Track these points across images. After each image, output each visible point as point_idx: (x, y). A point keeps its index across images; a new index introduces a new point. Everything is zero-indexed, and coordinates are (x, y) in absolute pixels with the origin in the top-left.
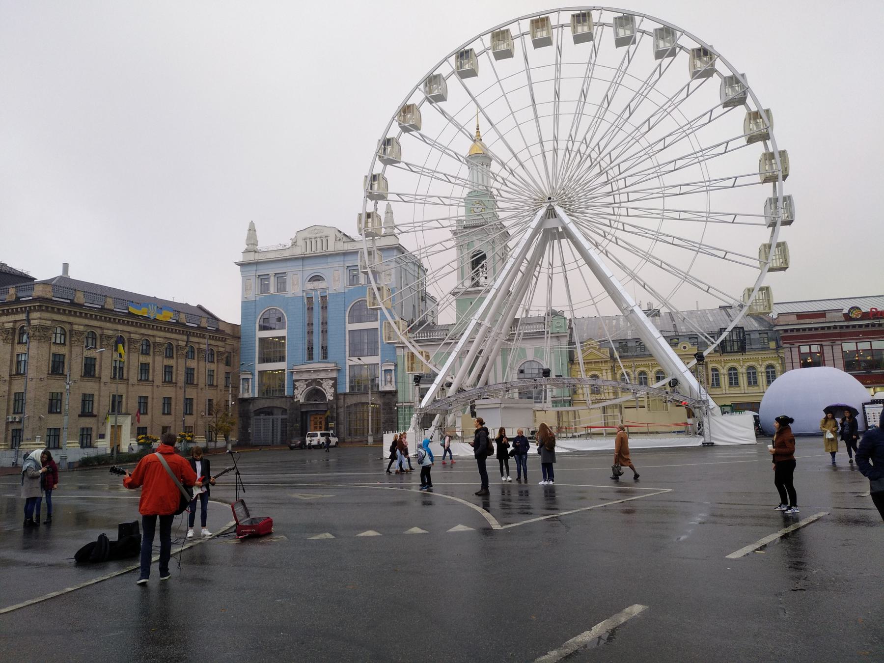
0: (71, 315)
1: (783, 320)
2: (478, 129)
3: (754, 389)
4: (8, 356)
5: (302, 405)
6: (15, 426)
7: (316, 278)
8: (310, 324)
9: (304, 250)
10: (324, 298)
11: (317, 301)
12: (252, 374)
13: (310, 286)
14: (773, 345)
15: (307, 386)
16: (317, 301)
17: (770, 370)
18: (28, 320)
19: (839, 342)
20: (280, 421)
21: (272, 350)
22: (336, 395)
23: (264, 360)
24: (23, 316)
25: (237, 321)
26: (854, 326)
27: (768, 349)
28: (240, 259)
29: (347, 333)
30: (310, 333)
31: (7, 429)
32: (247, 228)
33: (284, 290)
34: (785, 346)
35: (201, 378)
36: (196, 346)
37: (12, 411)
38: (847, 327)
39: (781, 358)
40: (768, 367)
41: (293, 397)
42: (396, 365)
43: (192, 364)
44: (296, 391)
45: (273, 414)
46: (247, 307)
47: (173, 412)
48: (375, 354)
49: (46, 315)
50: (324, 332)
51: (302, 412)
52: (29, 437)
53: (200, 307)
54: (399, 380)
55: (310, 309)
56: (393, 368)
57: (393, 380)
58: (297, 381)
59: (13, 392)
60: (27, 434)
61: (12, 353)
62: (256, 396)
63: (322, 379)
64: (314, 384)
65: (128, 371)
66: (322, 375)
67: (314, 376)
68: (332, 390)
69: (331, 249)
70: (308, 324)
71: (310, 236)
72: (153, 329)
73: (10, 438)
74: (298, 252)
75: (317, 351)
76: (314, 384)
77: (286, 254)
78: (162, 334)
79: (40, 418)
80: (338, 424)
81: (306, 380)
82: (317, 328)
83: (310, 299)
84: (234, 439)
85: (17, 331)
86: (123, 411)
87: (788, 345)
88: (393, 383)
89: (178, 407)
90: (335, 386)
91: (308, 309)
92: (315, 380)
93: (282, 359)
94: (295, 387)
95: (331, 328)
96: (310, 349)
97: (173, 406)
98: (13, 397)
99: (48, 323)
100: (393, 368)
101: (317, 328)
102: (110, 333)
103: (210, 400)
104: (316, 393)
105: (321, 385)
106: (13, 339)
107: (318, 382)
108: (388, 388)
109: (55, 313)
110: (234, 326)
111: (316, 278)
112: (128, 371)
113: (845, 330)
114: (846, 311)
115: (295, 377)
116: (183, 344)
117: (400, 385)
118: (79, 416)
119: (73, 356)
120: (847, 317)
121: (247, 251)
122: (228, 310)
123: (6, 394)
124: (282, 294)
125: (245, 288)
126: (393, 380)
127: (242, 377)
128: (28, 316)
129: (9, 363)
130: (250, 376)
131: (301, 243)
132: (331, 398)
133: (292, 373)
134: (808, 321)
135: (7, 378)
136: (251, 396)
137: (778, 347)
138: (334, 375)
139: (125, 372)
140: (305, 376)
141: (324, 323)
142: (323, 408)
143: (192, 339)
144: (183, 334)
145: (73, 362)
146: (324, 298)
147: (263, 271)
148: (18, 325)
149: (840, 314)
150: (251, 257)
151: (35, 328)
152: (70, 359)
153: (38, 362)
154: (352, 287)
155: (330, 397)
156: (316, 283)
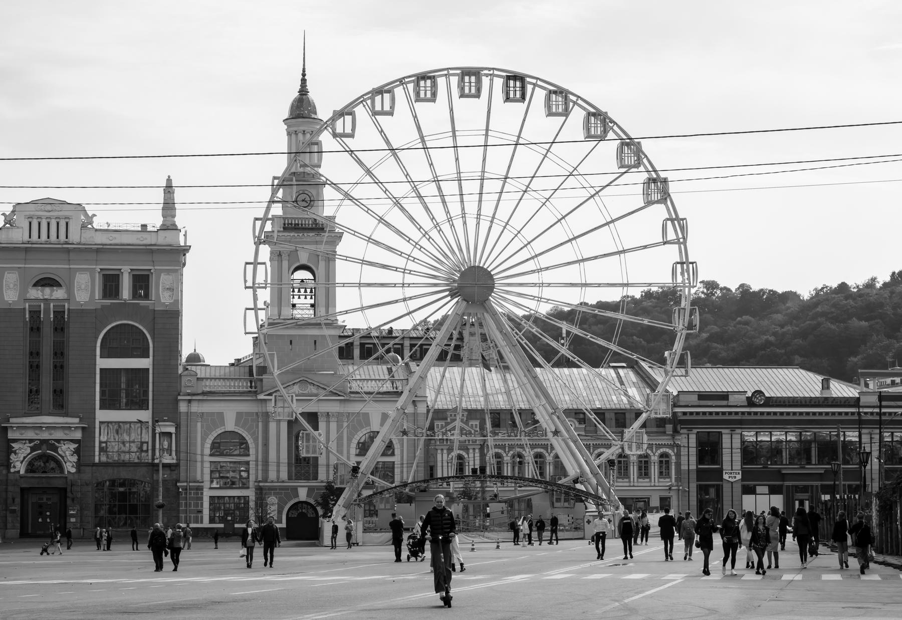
1: (683, 399)
3: (644, 482)
5: (21, 477)
8: (35, 353)
9: (26, 238)
10: (59, 314)
14: (669, 428)
15: (33, 449)
17: (664, 459)
19: (739, 431)
22: (79, 465)
26: (756, 413)
27: (664, 433)
29: (98, 372)
30: (35, 368)
34: (682, 431)
38: (749, 413)
39: (678, 446)
40: (662, 456)
42: (178, 428)
44: (13, 456)
48: (142, 405)
50: (59, 369)
51: (22, 490)
54: (183, 448)
56: (172, 430)
57: (174, 448)
63: (58, 441)
64: (44, 447)
66: (58, 435)
67: (45, 436)
68: (75, 459)
69: (74, 236)
74: (19, 236)
75: (47, 395)
80: (81, 510)
81: (31, 441)
82: (47, 361)
84: (73, 520)
87: (684, 431)
88: (174, 453)
90: (77, 452)
91: (32, 329)
92: (44, 442)
95: (73, 361)
96: (34, 393)
100: (172, 430)
101: (47, 361)
105: (55, 449)
107: (52, 445)
108: (167, 460)
113: (746, 417)
114: (749, 394)
117: (183, 455)
120: (750, 402)
126: (174, 448)
132: (73, 470)
134: (710, 403)
137: (676, 431)
138: (78, 435)
140: (30, 435)
141: (59, 353)
142: (59, 484)
146: (59, 314)
149: (743, 398)
154: (108, 302)
155: (70, 468)
156: (47, 290)
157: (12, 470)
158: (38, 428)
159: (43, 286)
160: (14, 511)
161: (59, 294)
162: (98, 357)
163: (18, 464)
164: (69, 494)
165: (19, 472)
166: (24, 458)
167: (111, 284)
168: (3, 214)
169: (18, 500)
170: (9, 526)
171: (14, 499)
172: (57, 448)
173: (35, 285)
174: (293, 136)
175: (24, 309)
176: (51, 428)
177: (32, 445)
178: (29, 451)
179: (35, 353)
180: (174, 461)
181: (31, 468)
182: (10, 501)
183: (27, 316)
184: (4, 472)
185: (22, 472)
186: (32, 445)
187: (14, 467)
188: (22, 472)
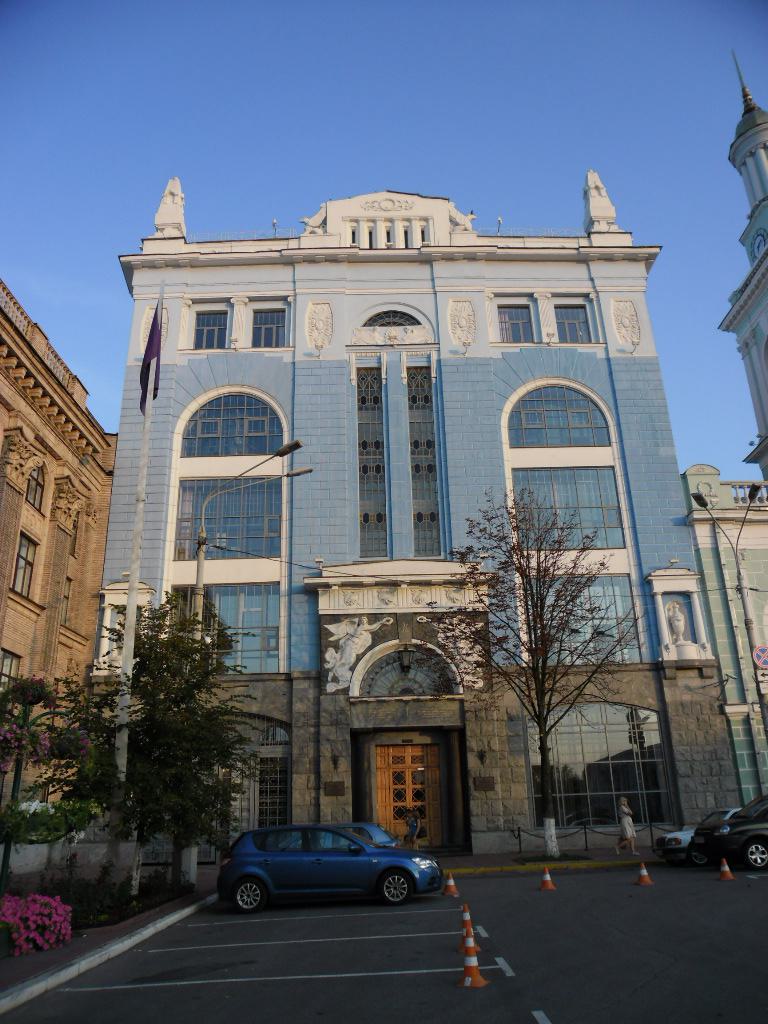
2: (745, 95)
13: (379, 335)
15: (377, 638)
29: (508, 474)
41: (320, 677)
42: (702, 581)
44: (330, 655)
58: (336, 619)
71: (372, 214)
81: (374, 617)
95: (457, 453)
100: (690, 585)
115: (326, 605)
140: (367, 602)
154: (514, 348)
157: (331, 688)
161: (415, 335)
162: (506, 446)
163: (343, 673)
164: (473, 744)
165: (346, 691)
166: (359, 658)
167: (518, 318)
169: (345, 765)
171: (335, 761)
174: (750, 161)
177: (376, 626)
179: (372, 446)
180: (709, 655)
185: (355, 692)
186: (376, 626)
187: (335, 680)
188: (355, 692)
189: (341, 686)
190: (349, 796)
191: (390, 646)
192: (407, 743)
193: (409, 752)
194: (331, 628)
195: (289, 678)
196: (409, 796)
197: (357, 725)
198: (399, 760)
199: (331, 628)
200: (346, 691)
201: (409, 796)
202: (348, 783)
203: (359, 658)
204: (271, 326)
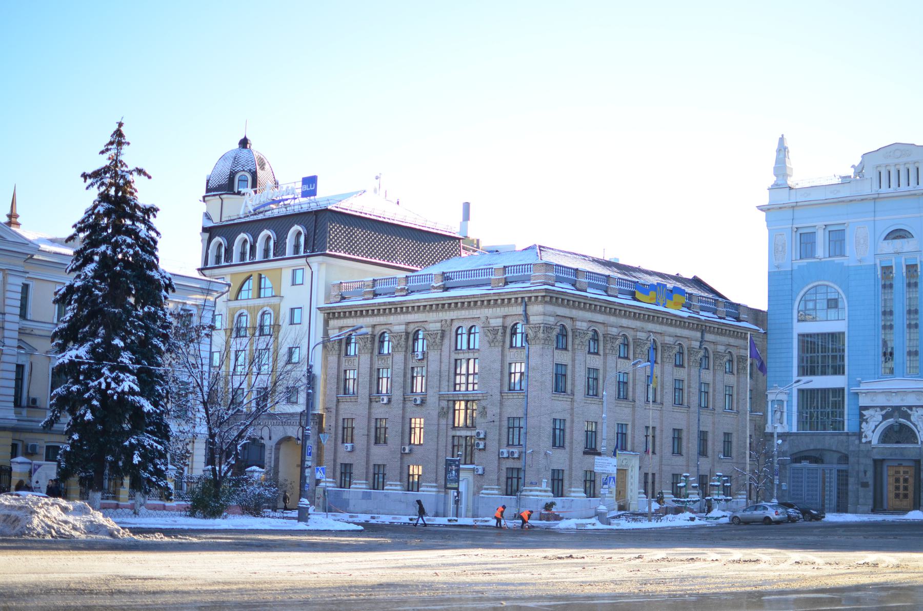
0: (574, 307)
4: (497, 366)
6: (510, 464)
7: (898, 234)
8: (888, 313)
10: (911, 268)
11: (899, 276)
12: (790, 394)
15: (885, 417)
16: (899, 276)
18: (526, 316)
20: (835, 475)
21: (822, 353)
23: (808, 369)
24: (519, 310)
25: (760, 303)
28: (765, 201)
31: (499, 469)
32: (775, 146)
33: (842, 254)
35: (719, 400)
36: (711, 348)
37: (505, 442)
41: (859, 435)
43: (707, 376)
44: (864, 425)
45: (822, 462)
46: (779, 282)
47: (684, 451)
49: (550, 308)
52: (534, 481)
53: (697, 282)
55: (888, 286)
58: (866, 408)
59: (506, 415)
60: (530, 476)
61: (502, 361)
62: (795, 430)
63: (910, 407)
64: (896, 414)
65: (634, 389)
66: (910, 400)
67: (896, 401)
70: (884, 313)
72: (662, 323)
73: (503, 479)
74: (868, 188)
76: (896, 414)
77: (845, 192)
78: (671, 330)
79: (546, 454)
81: (882, 408)
83: (887, 270)
85: (508, 331)
86: (629, 447)
89: (691, 444)
92: (897, 409)
93: (838, 370)
94: (862, 419)
97: (684, 443)
98: (505, 423)
99: (552, 320)
102: (614, 331)
103: (727, 435)
104: (899, 431)
105: (908, 417)
106: (504, 342)
109: (559, 305)
110: (757, 316)
111: (898, 234)
112: (634, 389)
115: (863, 401)
116: (696, 344)
118: (585, 453)
119: (577, 366)
121: (775, 187)
122: (749, 289)
123: (497, 419)
124: (837, 260)
125: (774, 250)
127: (771, 397)
128: (525, 311)
129: (499, 375)
130: (783, 397)
131: (870, 173)
133: (857, 394)
135: (498, 397)
136: (786, 430)
139: (630, 389)
140: (881, 401)
143: (709, 337)
144: (697, 329)
145: (577, 375)
147: (805, 221)
148: (509, 323)
150: (783, 197)
151: (537, 327)
152: (573, 372)
153: (542, 375)
156: (898, 244)
157: (864, 440)
158: (888, 393)
159: (895, 238)
160: (865, 485)
163: (869, 433)
165: (870, 442)
166: (876, 427)
168: (853, 166)
169: (870, 474)
170: (861, 501)
171: (865, 472)
172: (909, 415)
173: (885, 239)
175: (875, 265)
176: (904, 392)
178: (880, 418)
181: (886, 436)
182: (861, 474)
183: (879, 272)
184: (857, 442)
186: (884, 412)
187: (866, 437)
188: (875, 441)
189: (868, 439)
190: (871, 488)
191: (891, 421)
192: (900, 465)
193: (902, 470)
194: (864, 412)
195: (847, 434)
196: (901, 488)
197: (876, 457)
198: (898, 472)
199: (864, 412)
200: (870, 442)
201: (901, 488)
202: (871, 482)
203: (876, 427)
204: (837, 239)
